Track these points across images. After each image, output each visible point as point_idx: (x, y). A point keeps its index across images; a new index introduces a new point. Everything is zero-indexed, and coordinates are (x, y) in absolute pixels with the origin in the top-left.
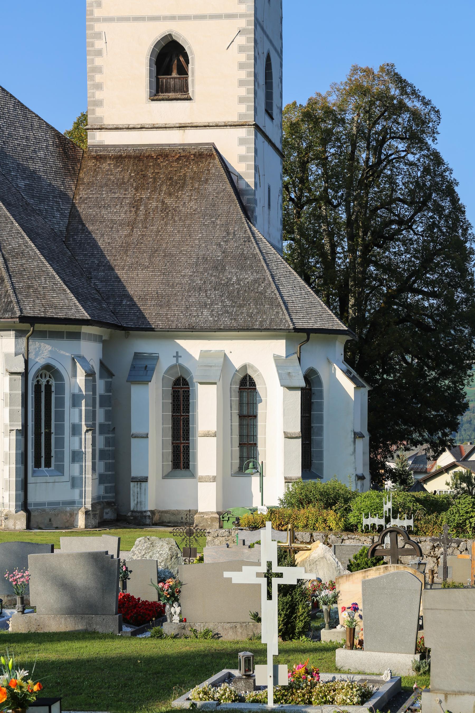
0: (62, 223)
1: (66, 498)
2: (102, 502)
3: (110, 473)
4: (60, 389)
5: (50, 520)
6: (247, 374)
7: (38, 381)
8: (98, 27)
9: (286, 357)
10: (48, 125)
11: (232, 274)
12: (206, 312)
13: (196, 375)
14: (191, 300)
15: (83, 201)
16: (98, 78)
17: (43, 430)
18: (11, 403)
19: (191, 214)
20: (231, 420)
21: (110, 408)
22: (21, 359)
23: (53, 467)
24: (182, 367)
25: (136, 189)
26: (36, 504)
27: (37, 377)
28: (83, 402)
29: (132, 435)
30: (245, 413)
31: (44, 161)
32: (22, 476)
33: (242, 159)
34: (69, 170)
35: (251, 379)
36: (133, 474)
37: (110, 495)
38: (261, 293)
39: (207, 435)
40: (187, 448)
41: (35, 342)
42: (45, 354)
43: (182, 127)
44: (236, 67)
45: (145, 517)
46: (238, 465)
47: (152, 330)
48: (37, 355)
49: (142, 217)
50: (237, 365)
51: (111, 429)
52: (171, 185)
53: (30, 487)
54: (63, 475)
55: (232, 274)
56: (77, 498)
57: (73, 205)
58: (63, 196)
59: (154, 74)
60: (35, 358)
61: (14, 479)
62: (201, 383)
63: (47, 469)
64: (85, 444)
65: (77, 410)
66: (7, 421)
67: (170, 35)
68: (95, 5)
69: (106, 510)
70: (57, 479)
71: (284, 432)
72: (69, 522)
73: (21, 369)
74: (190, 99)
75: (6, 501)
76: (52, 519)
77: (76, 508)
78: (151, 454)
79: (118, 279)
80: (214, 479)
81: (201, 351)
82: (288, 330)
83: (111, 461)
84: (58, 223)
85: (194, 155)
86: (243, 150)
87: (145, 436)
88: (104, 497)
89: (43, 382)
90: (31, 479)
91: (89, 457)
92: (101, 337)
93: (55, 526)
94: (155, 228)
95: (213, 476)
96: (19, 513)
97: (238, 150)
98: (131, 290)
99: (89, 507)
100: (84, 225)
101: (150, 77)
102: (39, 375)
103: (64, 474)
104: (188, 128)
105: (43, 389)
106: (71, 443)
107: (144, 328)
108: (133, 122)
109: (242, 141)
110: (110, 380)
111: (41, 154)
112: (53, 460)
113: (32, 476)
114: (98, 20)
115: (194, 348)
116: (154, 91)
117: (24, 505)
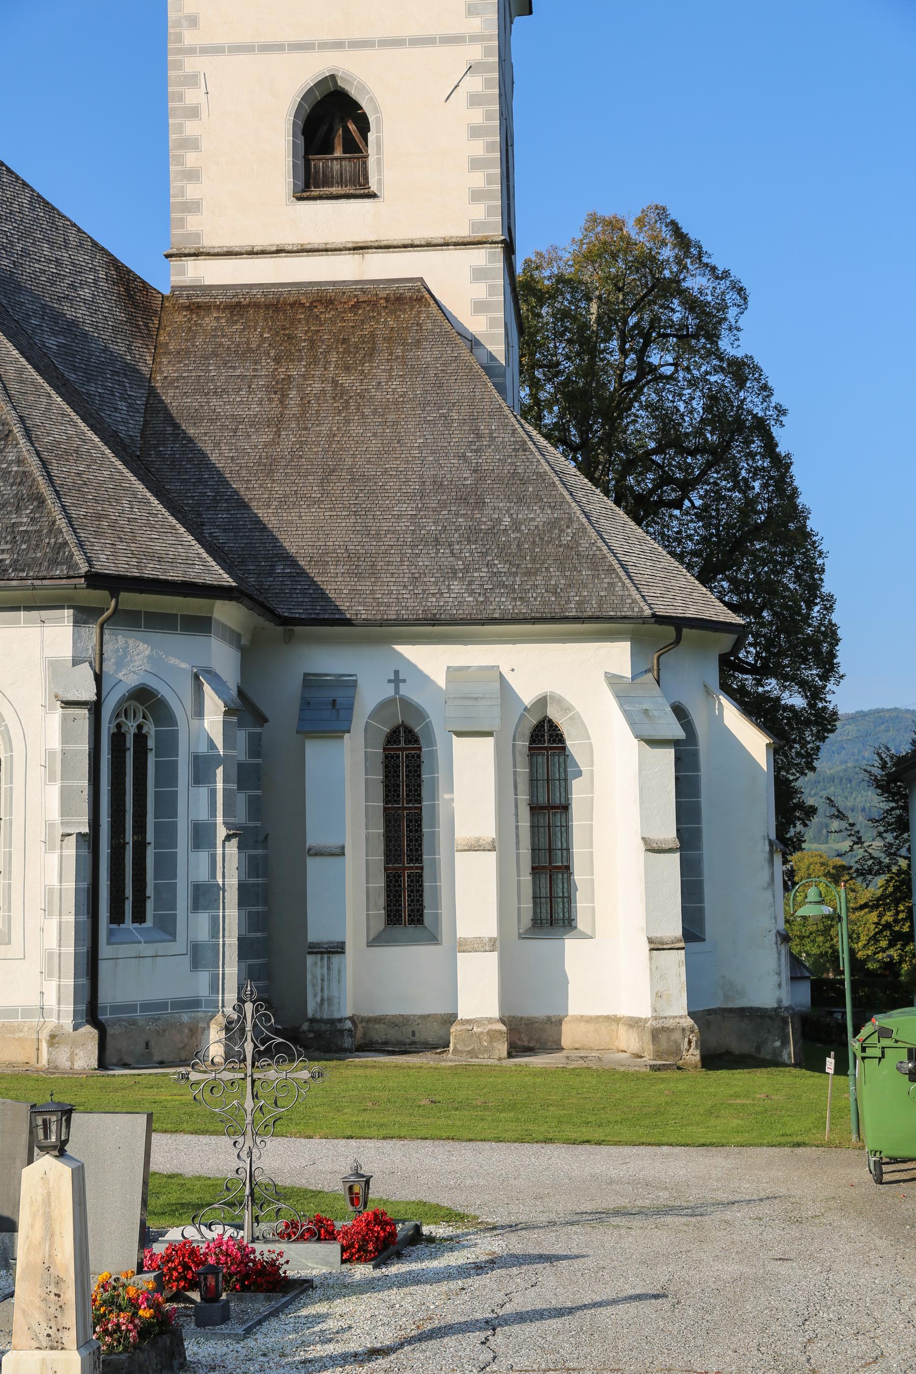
0: (131, 422)
1: (182, 992)
3: (259, 935)
4: (169, 744)
5: (147, 1044)
6: (546, 717)
7: (119, 726)
8: (192, 64)
9: (633, 678)
10: (95, 244)
11: (499, 510)
12: (456, 586)
13: (438, 722)
14: (420, 564)
15: (170, 382)
16: (191, 159)
17: (129, 837)
18: (66, 774)
19: (396, 403)
20: (517, 815)
21: (259, 792)
22: (86, 673)
23: (149, 923)
24: (406, 704)
25: (277, 360)
26: (116, 1009)
27: (118, 715)
28: (220, 772)
29: (310, 850)
30: (543, 800)
31: (91, 304)
32: (88, 942)
34: (138, 326)
38: (567, 546)
39: (475, 847)
40: (417, 880)
41: (116, 636)
42: (137, 663)
43: (359, 248)
44: (464, 133)
45: (342, 1031)
47: (348, 622)
48: (120, 665)
49: (295, 410)
50: (528, 698)
52: (347, 352)
55: (499, 510)
56: (203, 991)
57: (152, 391)
58: (131, 372)
60: (117, 672)
61: (71, 950)
62: (460, 734)
63: (137, 925)
64: (224, 867)
65: (203, 791)
66: (55, 814)
67: (333, 77)
68: (185, 23)
70: (161, 948)
71: (643, 838)
73: (89, 694)
74: (373, 196)
75: (51, 1001)
76: (152, 1043)
78: (345, 893)
79: (260, 526)
81: (448, 668)
82: (643, 620)
84: (125, 422)
85: (387, 299)
87: (338, 851)
89: (131, 727)
90: (105, 950)
91: (232, 897)
92: (239, 636)
93: (157, 1058)
94: (324, 429)
95: (490, 939)
97: (470, 294)
98: (291, 544)
100: (176, 426)
101: (295, 156)
102: (122, 711)
104: (370, 251)
105: (130, 742)
106: (191, 867)
107: (328, 619)
108: (260, 242)
110: (258, 730)
111: (86, 293)
112: (150, 905)
114: (191, 51)
115: (433, 662)
116: (301, 184)
117: (91, 1010)
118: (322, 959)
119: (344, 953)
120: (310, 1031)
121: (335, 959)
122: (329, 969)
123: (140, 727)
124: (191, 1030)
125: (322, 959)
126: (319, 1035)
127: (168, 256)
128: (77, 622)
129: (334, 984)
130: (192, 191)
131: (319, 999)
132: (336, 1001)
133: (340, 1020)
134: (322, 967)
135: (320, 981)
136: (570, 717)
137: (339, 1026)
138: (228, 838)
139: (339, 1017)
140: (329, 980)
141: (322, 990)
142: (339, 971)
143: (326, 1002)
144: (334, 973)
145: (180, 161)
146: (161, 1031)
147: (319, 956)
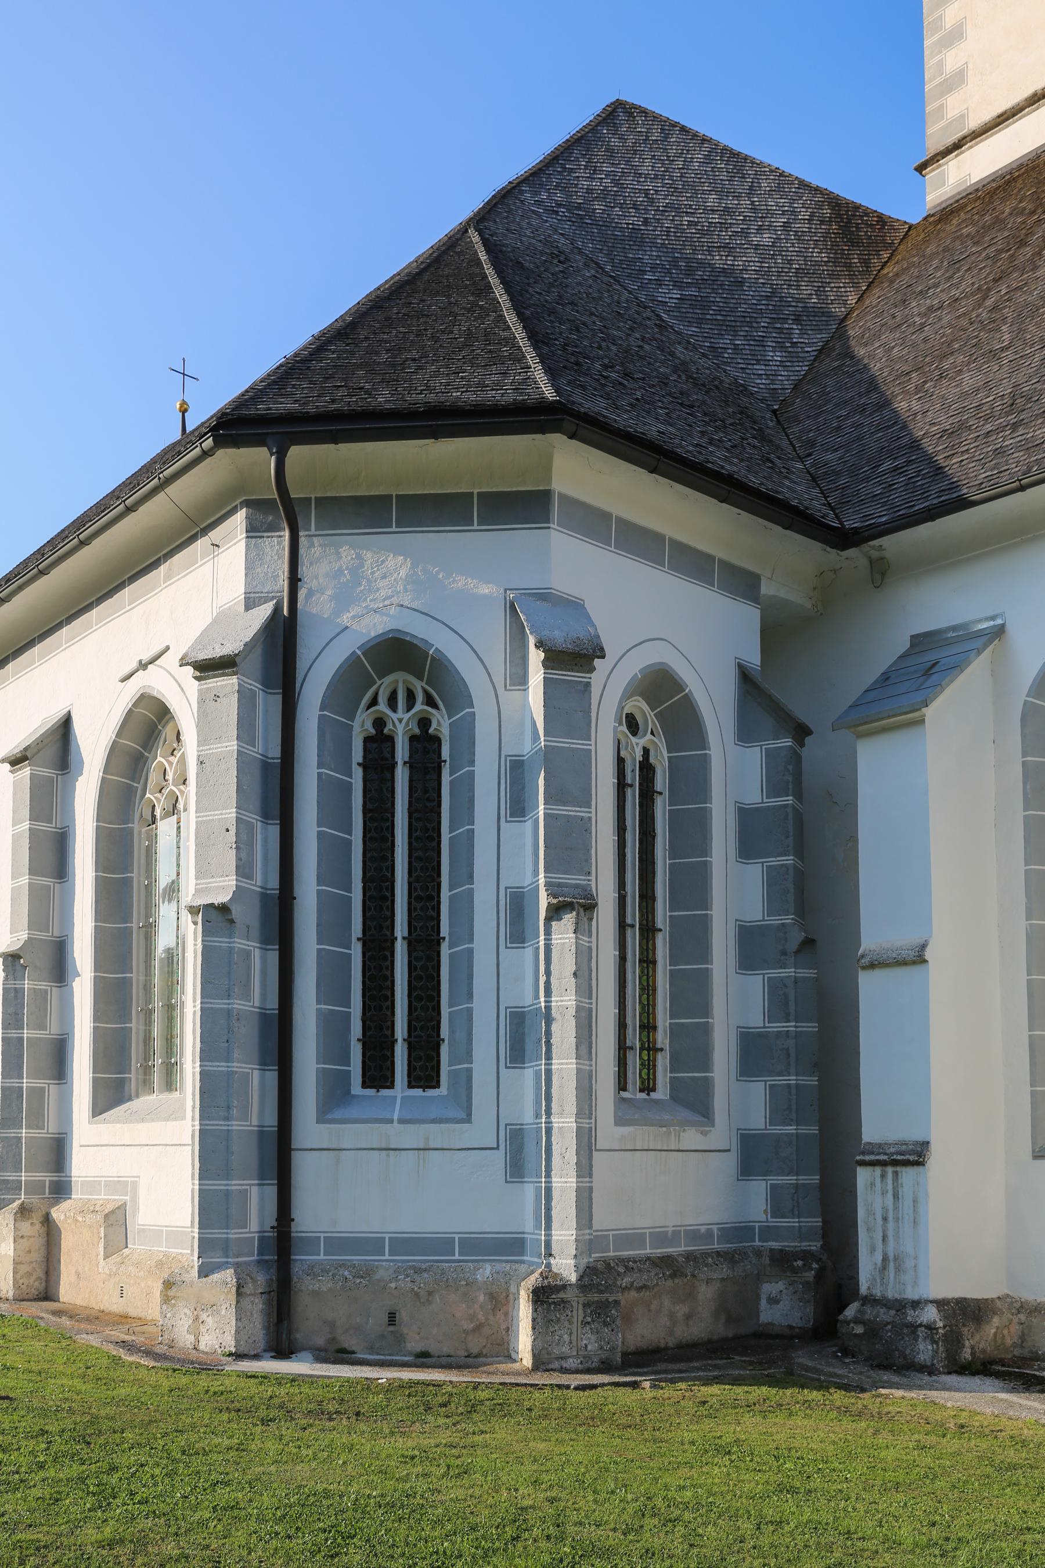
1: (488, 1221)
2: (758, 1253)
5: (392, 1318)
23: (443, 1090)
29: (863, 956)
36: (870, 1133)
37: (792, 1222)
51: (793, 944)
53: (307, 1169)
54: (468, 1119)
63: (418, 1092)
64: (548, 973)
69: (768, 1288)
70: (436, 1134)
72: (486, 1331)
76: (403, 1315)
77: (523, 1268)
83: (792, 1080)
87: (911, 955)
88: (767, 1232)
90: (308, 1127)
93: (415, 1344)
96: (216, 1277)
99: (566, 1267)
103: (469, 1114)
113: (319, 1121)
118: (883, 1176)
120: (857, 1321)
121: (908, 1174)
122: (896, 1196)
123: (424, 723)
124: (492, 1296)
125: (883, 1176)
126: (873, 1331)
128: (253, 530)
131: (878, 1257)
132: (909, 1264)
133: (916, 1304)
134: (884, 1193)
135: (880, 1222)
137: (911, 1316)
138: (555, 912)
139: (916, 1297)
140: (897, 1220)
141: (884, 1238)
142: (915, 1201)
143: (892, 1265)
146: (422, 1293)
147: (878, 1170)
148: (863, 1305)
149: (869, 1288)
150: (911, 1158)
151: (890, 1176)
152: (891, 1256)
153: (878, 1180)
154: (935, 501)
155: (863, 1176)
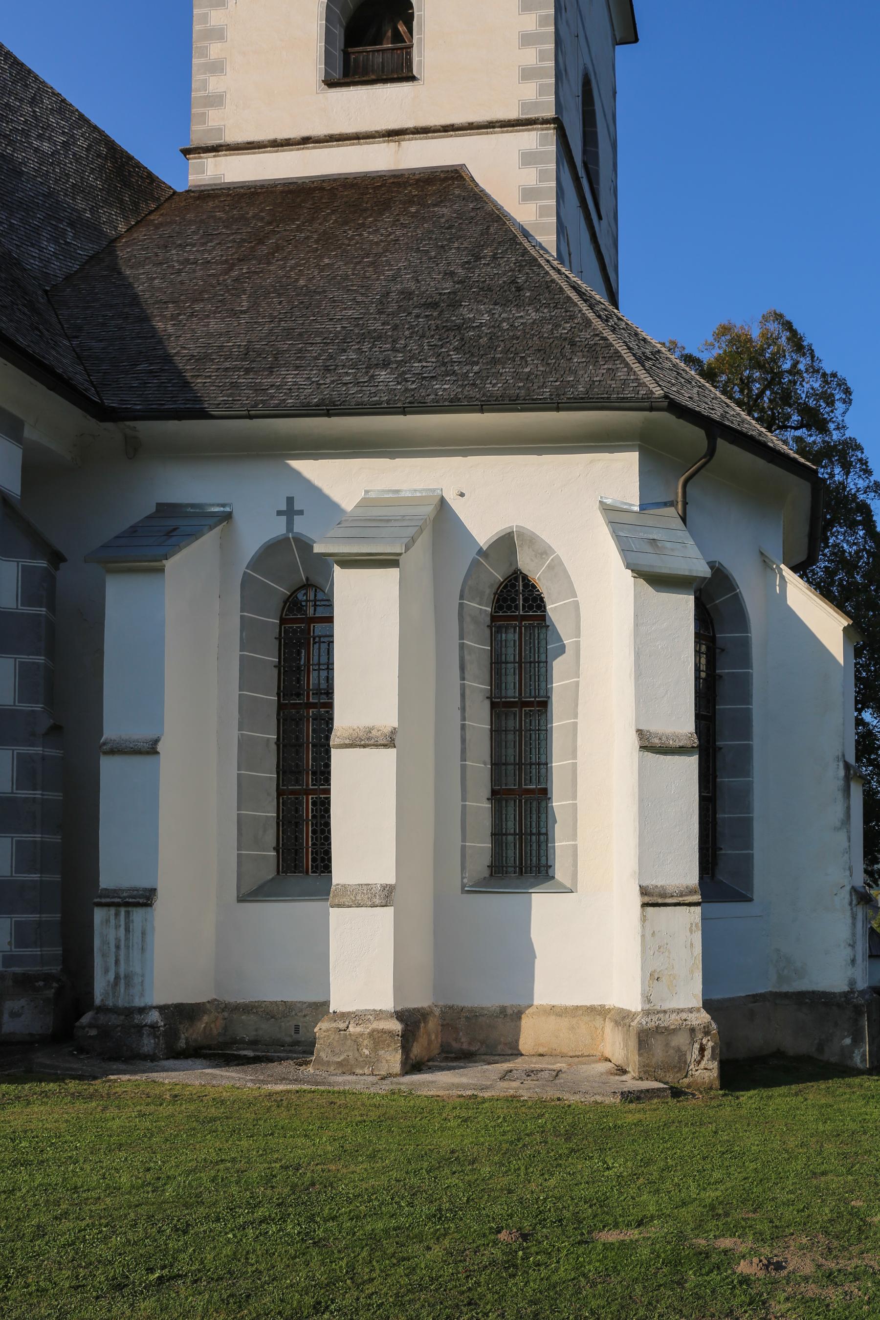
20: (463, 709)
30: (511, 693)
33: (528, 194)
35: (530, 587)
39: (364, 741)
43: (393, 134)
46: (486, 860)
59: (340, 42)
71: (638, 731)
74: (413, 78)
80: (387, 896)
86: (530, 177)
95: (384, 887)
104: (407, 137)
109: (528, 159)
115: (345, 482)
118: (117, 915)
119: (150, 905)
120: (91, 1026)
121: (138, 914)
122: (127, 930)
125: (117, 915)
127: (186, 152)
129: (136, 953)
130: (215, 84)
131: (111, 976)
134: (117, 927)
135: (113, 949)
136: (548, 566)
140: (127, 947)
141: (117, 962)
142: (143, 933)
143: (122, 981)
144: (136, 937)
145: (204, 53)
148: (97, 1013)
149: (102, 1000)
150: (141, 901)
151: (123, 914)
152: (122, 975)
153: (112, 918)
154: (182, 406)
155: (99, 915)
